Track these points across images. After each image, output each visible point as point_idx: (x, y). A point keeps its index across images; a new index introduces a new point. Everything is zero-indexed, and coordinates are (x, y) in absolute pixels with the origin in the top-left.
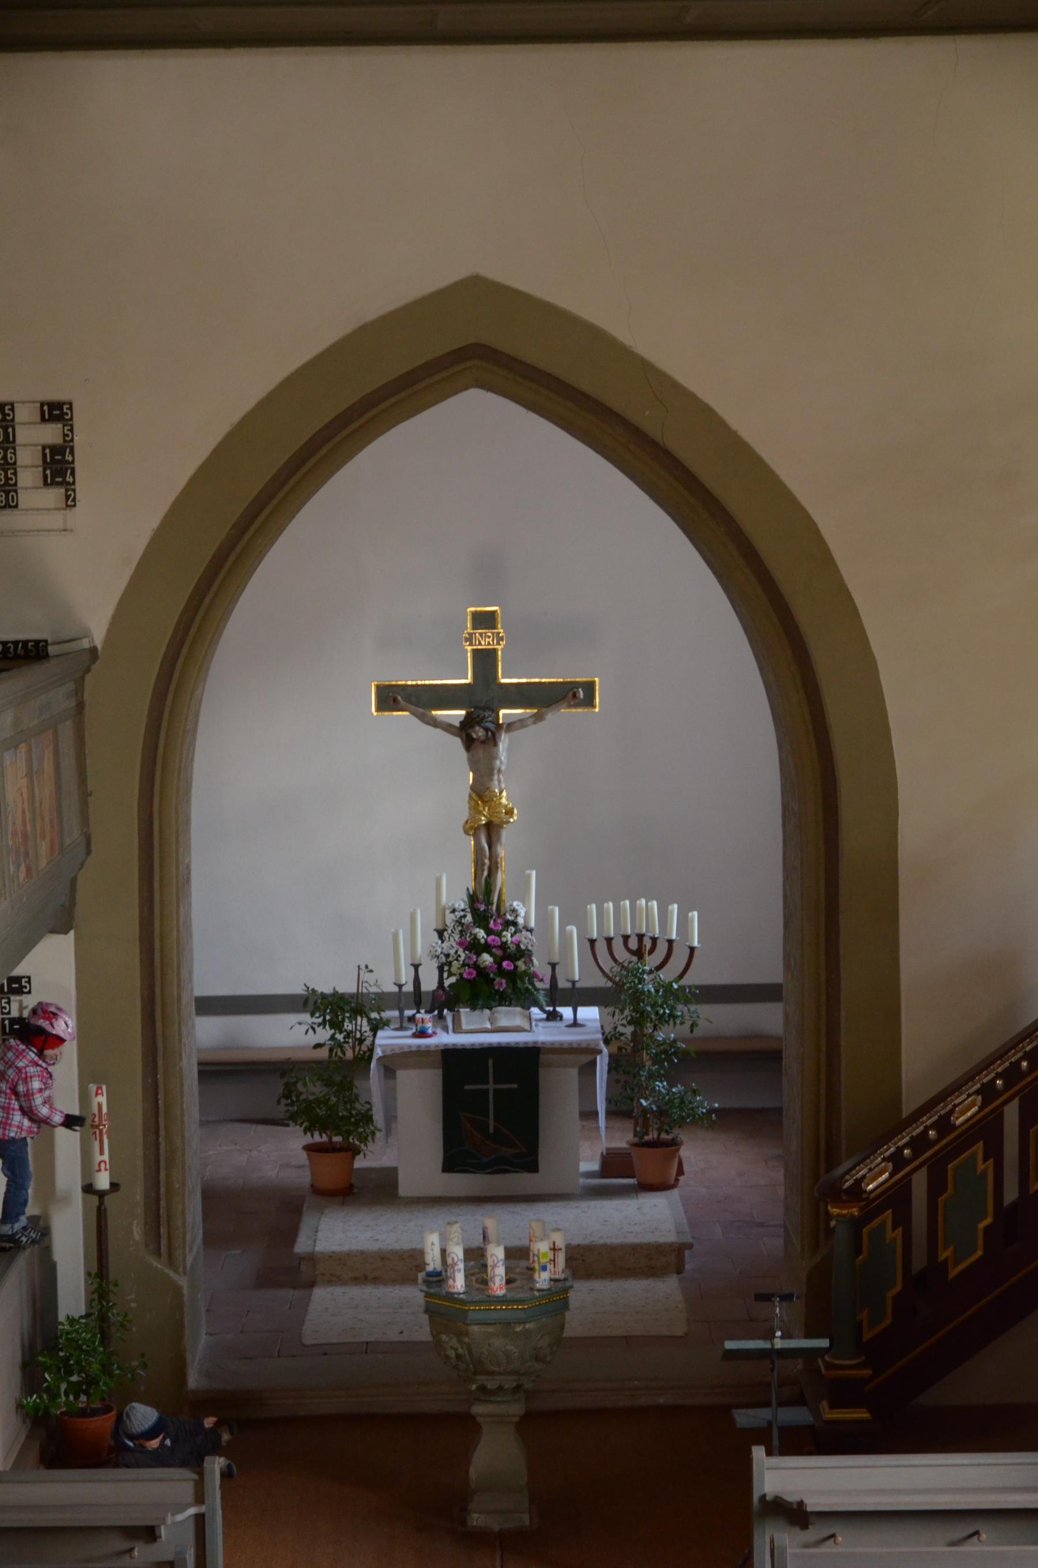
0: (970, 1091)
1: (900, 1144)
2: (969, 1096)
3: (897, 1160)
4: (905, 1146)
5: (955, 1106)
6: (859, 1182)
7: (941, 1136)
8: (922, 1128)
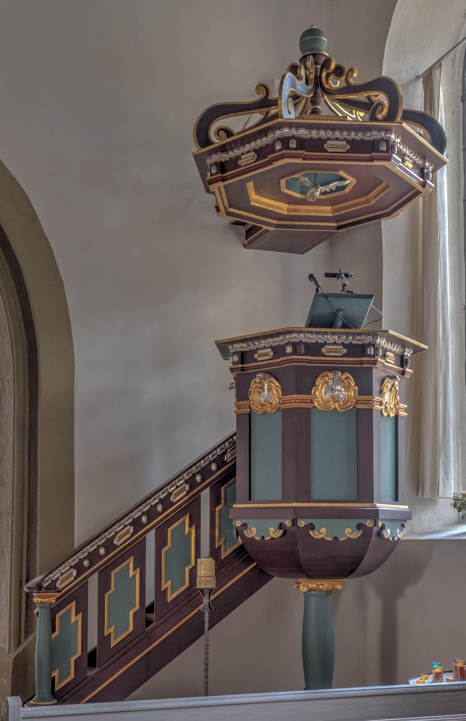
0: (126, 524)
1: (82, 557)
2: (125, 526)
3: (79, 568)
4: (85, 558)
5: (116, 533)
6: (54, 582)
7: (107, 553)
8: (95, 547)
